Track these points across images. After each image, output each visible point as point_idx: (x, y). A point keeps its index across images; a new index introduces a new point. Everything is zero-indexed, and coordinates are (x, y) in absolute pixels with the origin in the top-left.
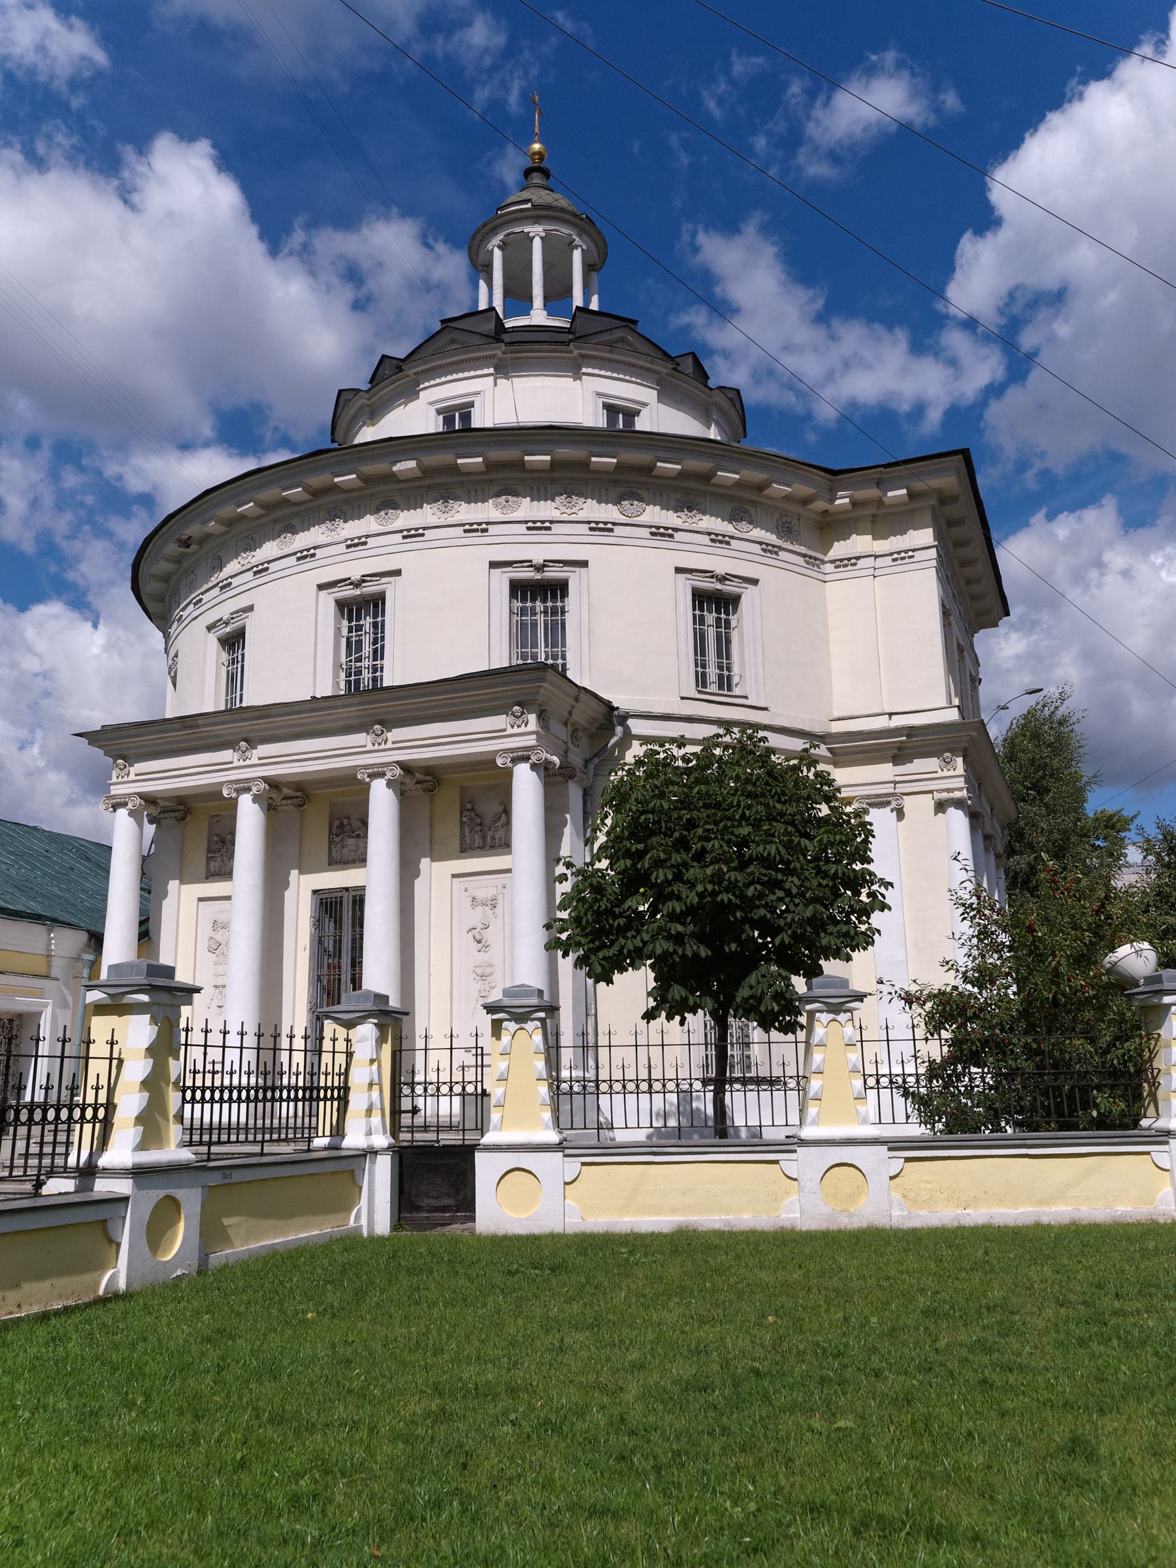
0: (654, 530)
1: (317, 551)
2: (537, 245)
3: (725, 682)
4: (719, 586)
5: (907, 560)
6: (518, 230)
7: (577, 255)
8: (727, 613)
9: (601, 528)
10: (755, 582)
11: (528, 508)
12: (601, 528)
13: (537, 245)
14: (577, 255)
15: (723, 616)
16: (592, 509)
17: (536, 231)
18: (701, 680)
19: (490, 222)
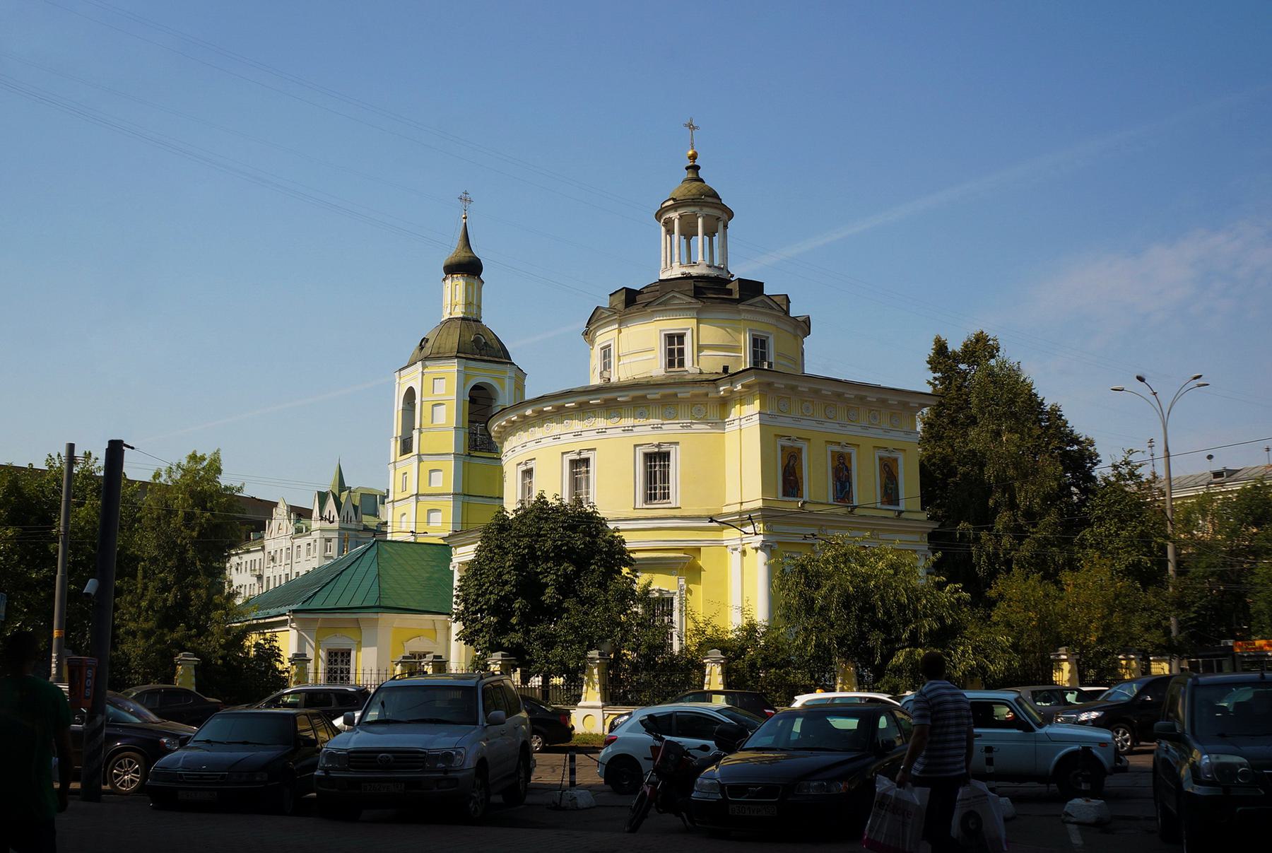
0: (623, 429)
1: (516, 449)
2: (676, 222)
3: (666, 496)
4: (656, 450)
5: (751, 421)
6: (667, 216)
7: (700, 220)
8: (664, 461)
9: (601, 431)
10: (677, 443)
11: (576, 425)
12: (601, 431)
13: (676, 222)
14: (700, 220)
15: (662, 463)
16: (600, 423)
17: (674, 215)
18: (650, 497)
19: (659, 211)
